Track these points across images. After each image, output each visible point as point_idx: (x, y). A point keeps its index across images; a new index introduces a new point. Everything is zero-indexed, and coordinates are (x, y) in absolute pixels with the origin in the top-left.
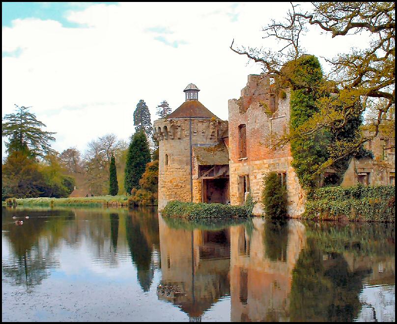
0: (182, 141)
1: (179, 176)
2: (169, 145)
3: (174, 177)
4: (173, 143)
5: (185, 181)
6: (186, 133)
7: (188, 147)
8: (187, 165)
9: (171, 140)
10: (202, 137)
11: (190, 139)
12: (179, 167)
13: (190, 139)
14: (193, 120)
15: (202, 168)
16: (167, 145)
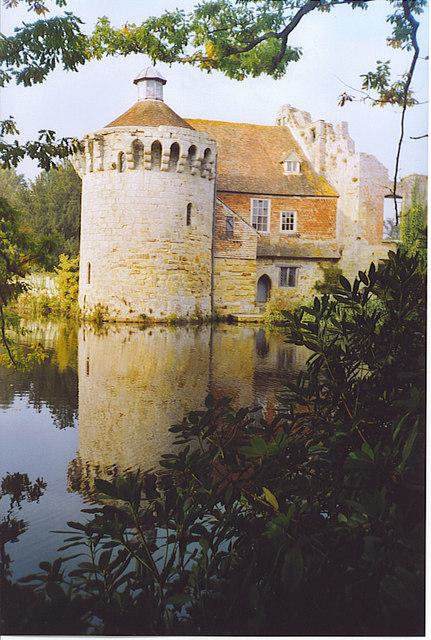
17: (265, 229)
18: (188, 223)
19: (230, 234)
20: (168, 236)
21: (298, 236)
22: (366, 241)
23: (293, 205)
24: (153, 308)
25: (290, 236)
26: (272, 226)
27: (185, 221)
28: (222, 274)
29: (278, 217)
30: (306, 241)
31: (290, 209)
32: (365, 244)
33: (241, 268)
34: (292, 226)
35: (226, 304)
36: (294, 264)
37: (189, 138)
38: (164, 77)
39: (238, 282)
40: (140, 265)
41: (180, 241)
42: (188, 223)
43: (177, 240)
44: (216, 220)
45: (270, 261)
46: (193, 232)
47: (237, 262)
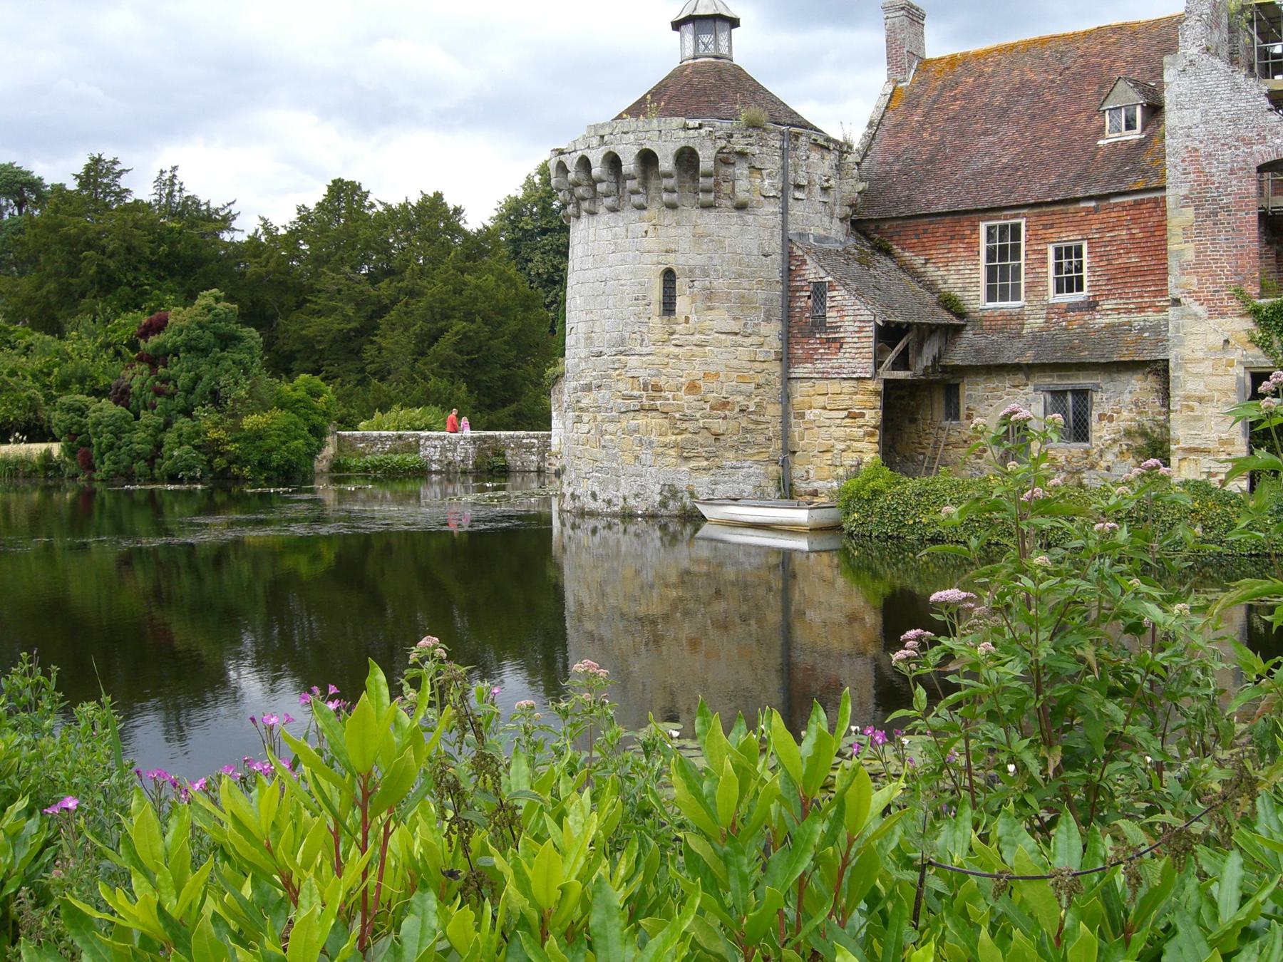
0: (750, 218)
1: (735, 363)
2: (686, 231)
3: (712, 369)
4: (708, 220)
5: (759, 386)
6: (769, 185)
7: (775, 245)
8: (768, 319)
9: (698, 211)
10: (820, 207)
11: (785, 212)
12: (735, 326)
13: (785, 212)
14: (797, 136)
15: (888, 334)
16: (672, 232)
17: (1016, 297)
18: (668, 306)
19: (819, 323)
20: (622, 342)
21: (1092, 306)
22: (1197, 309)
23: (1077, 225)
24: (597, 489)
25: (1073, 307)
26: (1030, 287)
27: (656, 308)
28: (809, 415)
29: (1044, 262)
30: (1113, 318)
31: (1070, 237)
32: (1196, 317)
33: (845, 401)
34: (1080, 279)
35: (816, 485)
36: (1082, 381)
37: (632, 137)
38: (733, 12)
39: (840, 432)
40: (585, 402)
41: (645, 350)
42: (668, 306)
43: (638, 349)
44: (790, 293)
45: (1021, 376)
46: (678, 328)
47: (834, 387)
